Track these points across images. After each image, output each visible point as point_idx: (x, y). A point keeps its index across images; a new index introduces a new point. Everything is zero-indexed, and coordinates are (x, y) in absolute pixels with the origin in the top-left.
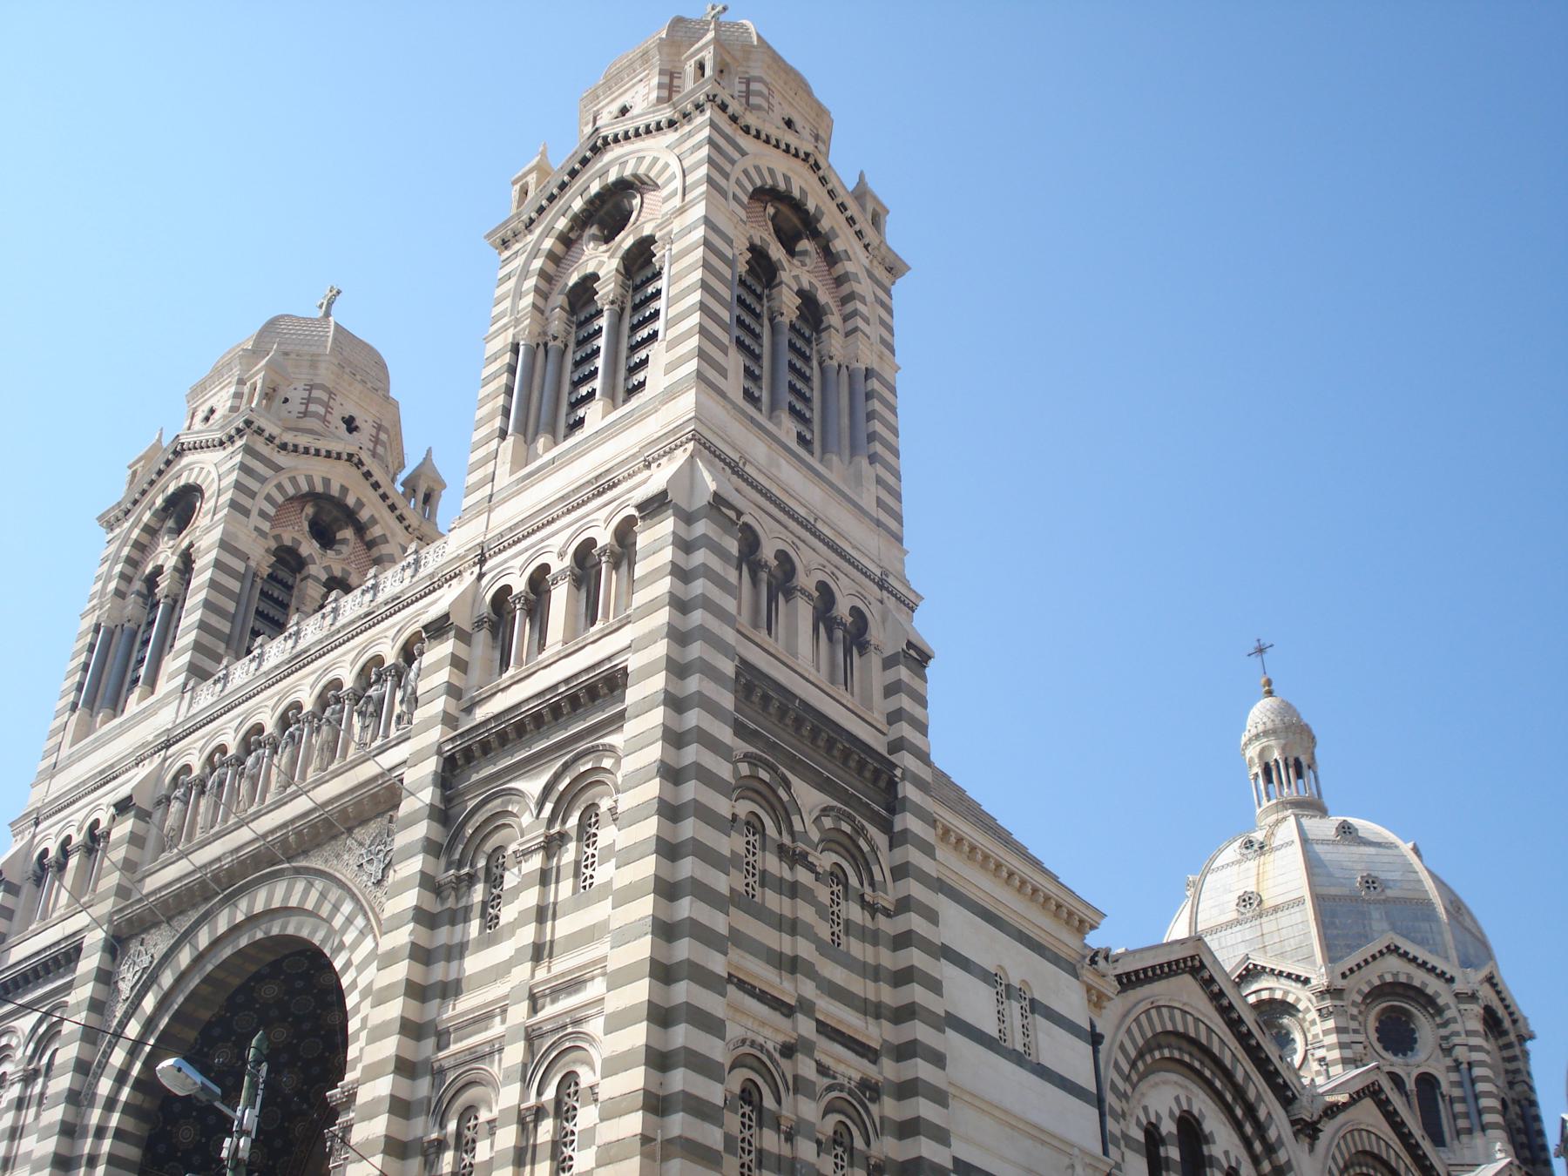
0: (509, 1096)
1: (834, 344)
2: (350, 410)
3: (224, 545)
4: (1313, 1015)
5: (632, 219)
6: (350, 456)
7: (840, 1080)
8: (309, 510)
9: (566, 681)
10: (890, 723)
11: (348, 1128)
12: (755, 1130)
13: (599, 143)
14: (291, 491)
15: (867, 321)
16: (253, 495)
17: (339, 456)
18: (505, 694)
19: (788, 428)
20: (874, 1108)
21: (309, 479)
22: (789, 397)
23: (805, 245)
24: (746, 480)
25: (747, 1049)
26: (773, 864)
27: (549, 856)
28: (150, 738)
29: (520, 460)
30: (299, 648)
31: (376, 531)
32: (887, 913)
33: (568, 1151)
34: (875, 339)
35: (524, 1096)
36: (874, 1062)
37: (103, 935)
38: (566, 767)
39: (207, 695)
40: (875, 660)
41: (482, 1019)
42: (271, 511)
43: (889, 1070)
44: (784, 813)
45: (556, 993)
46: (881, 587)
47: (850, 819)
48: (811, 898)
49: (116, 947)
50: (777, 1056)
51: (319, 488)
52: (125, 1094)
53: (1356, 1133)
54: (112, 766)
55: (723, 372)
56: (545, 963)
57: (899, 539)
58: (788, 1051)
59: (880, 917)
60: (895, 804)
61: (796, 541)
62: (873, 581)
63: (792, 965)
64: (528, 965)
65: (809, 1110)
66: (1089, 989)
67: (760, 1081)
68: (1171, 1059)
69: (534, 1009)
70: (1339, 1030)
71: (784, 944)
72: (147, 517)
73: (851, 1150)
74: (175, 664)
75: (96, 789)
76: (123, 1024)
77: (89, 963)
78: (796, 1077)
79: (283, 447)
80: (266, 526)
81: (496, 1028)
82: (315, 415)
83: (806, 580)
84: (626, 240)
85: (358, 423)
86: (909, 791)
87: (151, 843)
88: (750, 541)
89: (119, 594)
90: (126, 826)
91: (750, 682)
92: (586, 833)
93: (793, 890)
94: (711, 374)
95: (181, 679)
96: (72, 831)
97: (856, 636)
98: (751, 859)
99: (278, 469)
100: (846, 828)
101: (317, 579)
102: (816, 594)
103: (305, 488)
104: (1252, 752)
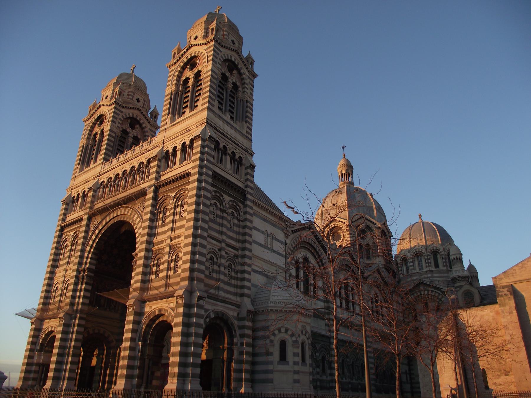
0: (166, 257)
1: (240, 95)
2: (138, 97)
3: (110, 130)
4: (345, 230)
5: (197, 65)
6: (138, 108)
7: (230, 255)
8: (129, 121)
9: (179, 174)
10: (246, 181)
11: (136, 261)
12: (212, 265)
13: (191, 46)
14: (125, 117)
15: (247, 89)
16: (116, 118)
17: (135, 109)
19: (227, 117)
20: (237, 260)
21: (129, 114)
22: (229, 108)
23: (235, 72)
24: (217, 131)
25: (211, 250)
26: (219, 213)
28: (96, 174)
29: (172, 120)
30: (126, 158)
31: (144, 125)
32: (242, 221)
33: (177, 269)
34: (249, 94)
35: (169, 258)
36: (237, 251)
37: (87, 217)
39: (107, 166)
40: (243, 168)
41: (161, 242)
42: (120, 122)
43: (240, 252)
44: (221, 202)
45: (176, 238)
46: (246, 152)
47: (235, 202)
48: (226, 219)
49: (89, 219)
50: (217, 251)
51: (131, 116)
52: (92, 250)
53: (343, 261)
55: (213, 106)
56: (173, 231)
57: (251, 140)
58: (220, 250)
59: (241, 222)
60: (245, 199)
61: (228, 143)
62: (244, 150)
63: (221, 233)
64: (170, 232)
65: (223, 261)
66: (285, 234)
67: (214, 256)
68: (303, 247)
69: (171, 241)
70: (350, 234)
71: (220, 229)
72: (93, 121)
73: (231, 268)
74: (101, 157)
76: (92, 236)
77: (84, 222)
78: (221, 255)
79: (123, 107)
80: (119, 126)
81: (164, 244)
82: (130, 99)
83: (229, 152)
84: (195, 70)
85: (140, 100)
86: (249, 196)
87: (97, 197)
88: (217, 143)
89: (88, 138)
90: (91, 194)
91: (216, 176)
92: (182, 205)
93: (222, 218)
94: (211, 107)
95: (102, 161)
96: (80, 192)
97: (239, 162)
98: (214, 212)
99: (122, 112)
100: (235, 204)
101: (131, 137)
102: (231, 154)
103: (128, 116)
104: (339, 171)
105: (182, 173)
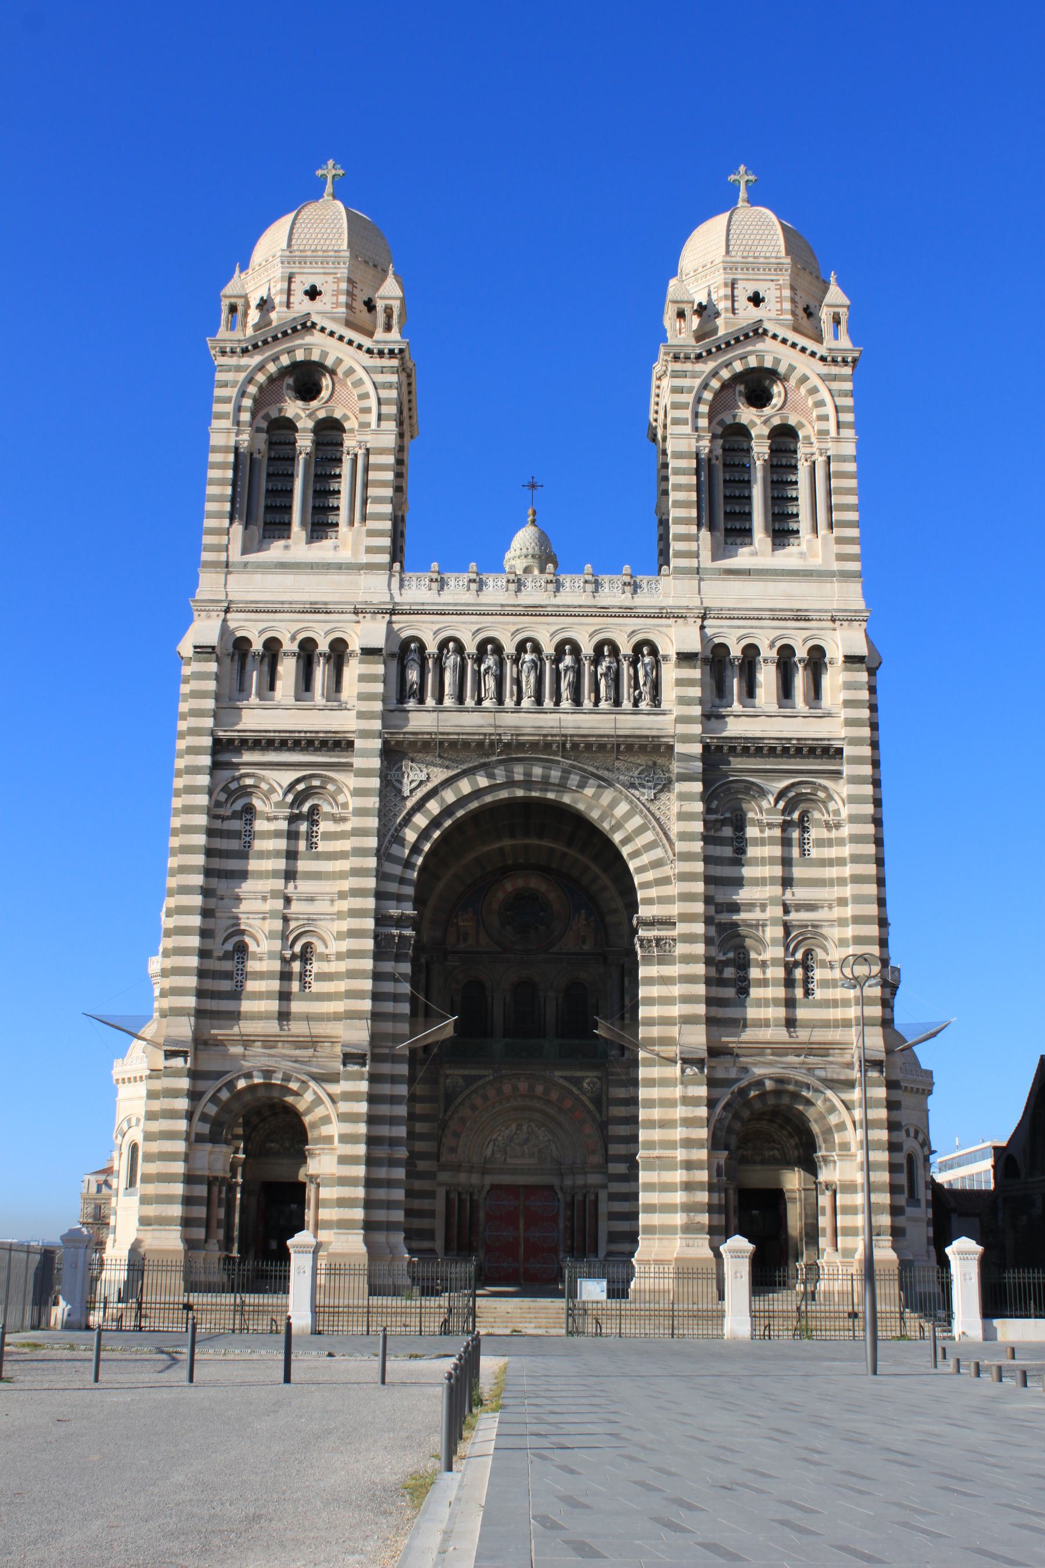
18: (736, 719)
27: (783, 831)
38: (793, 785)
54: (326, 603)
75: (303, 612)
105: (810, 742)
